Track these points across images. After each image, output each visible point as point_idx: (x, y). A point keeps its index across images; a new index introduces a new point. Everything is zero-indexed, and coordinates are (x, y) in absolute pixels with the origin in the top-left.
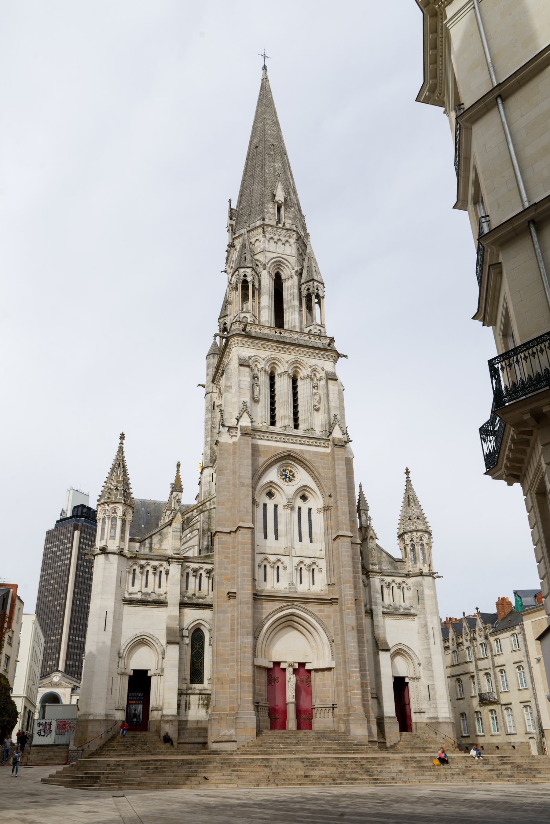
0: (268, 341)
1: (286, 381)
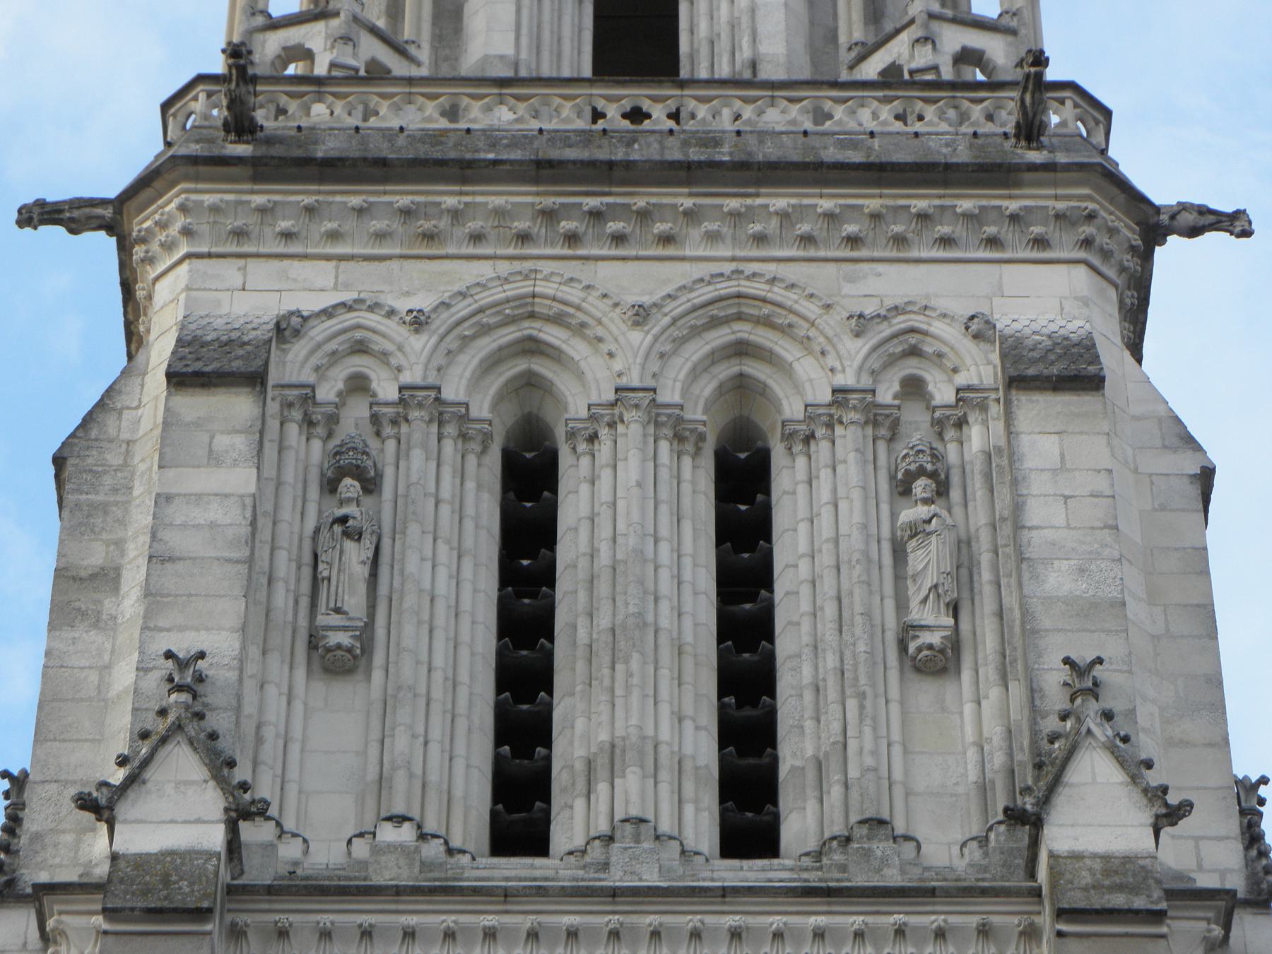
0: (464, 181)
1: (631, 469)
